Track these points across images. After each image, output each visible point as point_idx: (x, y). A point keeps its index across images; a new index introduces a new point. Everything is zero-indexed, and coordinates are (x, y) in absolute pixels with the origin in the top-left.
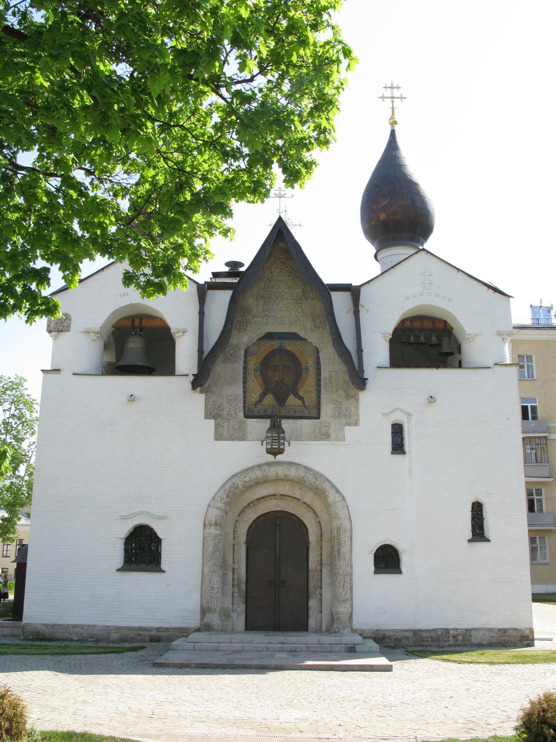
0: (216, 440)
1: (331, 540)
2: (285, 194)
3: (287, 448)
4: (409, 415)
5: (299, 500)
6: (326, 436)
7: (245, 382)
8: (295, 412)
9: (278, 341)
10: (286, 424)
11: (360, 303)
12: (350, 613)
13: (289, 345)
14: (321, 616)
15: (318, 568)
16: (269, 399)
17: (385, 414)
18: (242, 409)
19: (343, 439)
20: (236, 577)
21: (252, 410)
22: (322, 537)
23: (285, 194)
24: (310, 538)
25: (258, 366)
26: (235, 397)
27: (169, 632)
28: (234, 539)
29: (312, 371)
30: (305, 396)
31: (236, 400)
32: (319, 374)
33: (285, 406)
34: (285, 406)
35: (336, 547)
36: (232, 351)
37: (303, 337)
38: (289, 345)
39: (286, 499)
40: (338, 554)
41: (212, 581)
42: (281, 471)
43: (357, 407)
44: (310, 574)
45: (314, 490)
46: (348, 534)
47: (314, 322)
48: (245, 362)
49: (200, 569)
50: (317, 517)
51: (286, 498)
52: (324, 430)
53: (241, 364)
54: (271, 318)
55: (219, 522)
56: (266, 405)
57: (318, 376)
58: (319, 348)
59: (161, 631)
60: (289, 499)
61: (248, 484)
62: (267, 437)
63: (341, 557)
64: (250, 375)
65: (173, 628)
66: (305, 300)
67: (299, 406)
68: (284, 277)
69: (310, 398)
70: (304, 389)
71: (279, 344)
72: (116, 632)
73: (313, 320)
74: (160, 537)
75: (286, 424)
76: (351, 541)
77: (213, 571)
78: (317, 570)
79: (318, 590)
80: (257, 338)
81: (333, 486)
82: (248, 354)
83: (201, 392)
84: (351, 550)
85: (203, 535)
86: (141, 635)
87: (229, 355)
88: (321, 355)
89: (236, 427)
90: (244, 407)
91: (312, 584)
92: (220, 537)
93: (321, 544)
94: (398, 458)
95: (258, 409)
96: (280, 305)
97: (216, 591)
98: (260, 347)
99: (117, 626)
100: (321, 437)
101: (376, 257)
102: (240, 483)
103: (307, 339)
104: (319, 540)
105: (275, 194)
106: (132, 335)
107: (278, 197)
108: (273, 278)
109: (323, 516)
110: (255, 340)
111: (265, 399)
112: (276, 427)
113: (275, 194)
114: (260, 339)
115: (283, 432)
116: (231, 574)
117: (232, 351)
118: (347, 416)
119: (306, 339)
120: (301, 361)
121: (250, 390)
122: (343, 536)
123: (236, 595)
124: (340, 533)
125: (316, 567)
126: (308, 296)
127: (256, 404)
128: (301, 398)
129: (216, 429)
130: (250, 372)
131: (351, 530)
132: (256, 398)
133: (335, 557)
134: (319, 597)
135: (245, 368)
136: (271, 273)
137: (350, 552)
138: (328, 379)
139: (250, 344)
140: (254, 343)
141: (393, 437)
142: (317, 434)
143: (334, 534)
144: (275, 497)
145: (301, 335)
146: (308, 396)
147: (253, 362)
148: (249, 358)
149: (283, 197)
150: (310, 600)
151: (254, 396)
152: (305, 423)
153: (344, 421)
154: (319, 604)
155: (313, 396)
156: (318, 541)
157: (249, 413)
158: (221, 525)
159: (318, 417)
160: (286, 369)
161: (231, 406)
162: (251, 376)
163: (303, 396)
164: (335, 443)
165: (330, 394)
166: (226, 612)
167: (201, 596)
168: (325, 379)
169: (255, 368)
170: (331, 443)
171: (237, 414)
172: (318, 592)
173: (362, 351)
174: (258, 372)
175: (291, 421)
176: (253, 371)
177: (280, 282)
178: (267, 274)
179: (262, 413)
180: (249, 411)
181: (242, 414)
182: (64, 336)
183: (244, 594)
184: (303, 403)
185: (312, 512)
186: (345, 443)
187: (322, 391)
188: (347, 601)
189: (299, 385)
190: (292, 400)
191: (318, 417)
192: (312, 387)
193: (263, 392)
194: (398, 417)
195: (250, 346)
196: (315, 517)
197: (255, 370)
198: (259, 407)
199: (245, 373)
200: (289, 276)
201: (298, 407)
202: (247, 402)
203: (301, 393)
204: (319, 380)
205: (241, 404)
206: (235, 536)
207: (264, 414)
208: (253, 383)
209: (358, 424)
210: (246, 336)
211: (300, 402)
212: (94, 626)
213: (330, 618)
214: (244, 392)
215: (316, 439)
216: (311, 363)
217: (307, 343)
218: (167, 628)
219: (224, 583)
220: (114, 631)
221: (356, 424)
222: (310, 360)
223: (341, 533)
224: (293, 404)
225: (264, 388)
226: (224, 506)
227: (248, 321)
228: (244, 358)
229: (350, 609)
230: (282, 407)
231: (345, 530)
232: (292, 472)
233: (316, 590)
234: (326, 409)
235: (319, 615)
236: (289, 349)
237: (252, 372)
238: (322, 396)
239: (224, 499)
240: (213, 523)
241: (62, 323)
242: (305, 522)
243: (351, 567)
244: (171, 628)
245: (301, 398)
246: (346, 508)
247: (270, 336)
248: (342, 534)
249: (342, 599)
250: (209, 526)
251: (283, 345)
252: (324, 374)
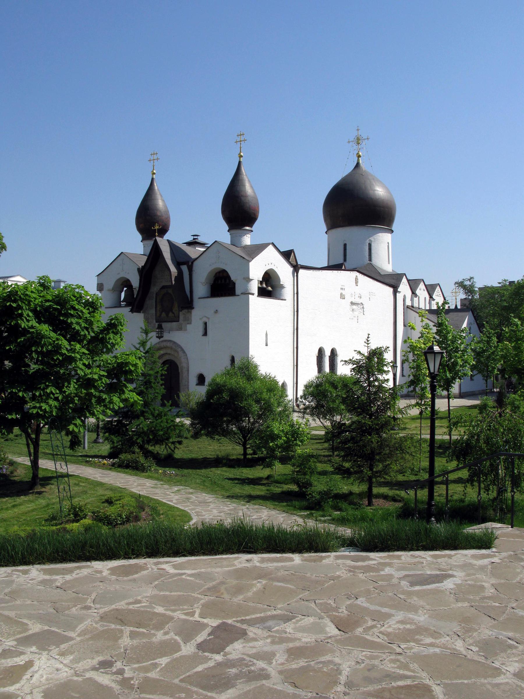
4: (208, 318)
6: (180, 329)
10: (164, 325)
16: (164, 314)
17: (200, 319)
19: (186, 330)
42: (165, 344)
43: (191, 316)
48: (156, 299)
53: (154, 300)
75: (164, 325)
81: (182, 350)
84: (188, 376)
94: (205, 337)
112: (160, 327)
128: (173, 313)
135: (156, 302)
152: (174, 324)
159: (178, 321)
175: (170, 323)
181: (155, 321)
182: (103, 292)
190: (171, 314)
191: (178, 321)
194: (205, 320)
205: (154, 317)
211: (173, 315)
215: (177, 330)
221: (190, 323)
232: (169, 344)
234: (181, 317)
243: (188, 382)
245: (173, 313)
247: (163, 287)
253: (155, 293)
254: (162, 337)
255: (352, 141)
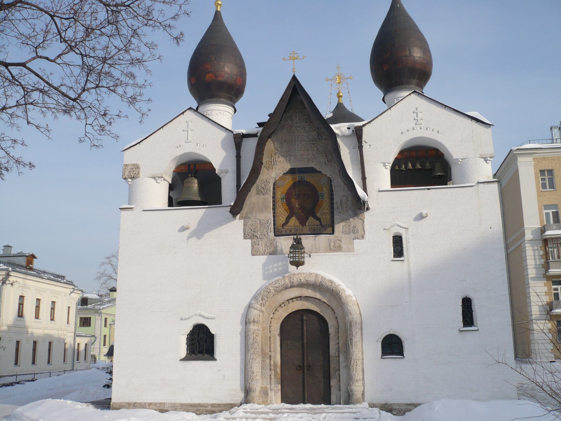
0: (253, 255)
1: (346, 331)
2: (298, 56)
3: (307, 260)
5: (320, 300)
6: (339, 248)
7: (274, 209)
8: (314, 230)
9: (299, 175)
10: (307, 241)
11: (363, 140)
12: (362, 390)
13: (307, 178)
14: (340, 393)
15: (337, 355)
16: (294, 221)
18: (273, 229)
20: (272, 363)
21: (280, 230)
22: (338, 329)
23: (298, 56)
24: (330, 330)
25: (284, 195)
26: (267, 221)
27: (221, 407)
28: (270, 333)
29: (326, 198)
30: (322, 217)
31: (267, 223)
32: (332, 199)
33: (306, 226)
34: (306, 226)
35: (349, 337)
36: (263, 185)
37: (319, 170)
38: (307, 178)
39: (310, 300)
40: (351, 343)
41: (252, 367)
44: (331, 359)
45: (330, 292)
46: (358, 326)
47: (326, 158)
48: (274, 193)
49: (244, 356)
50: (335, 313)
51: (310, 299)
52: (337, 244)
54: (293, 157)
55: (256, 320)
56: (291, 226)
57: (331, 201)
58: (332, 179)
59: (215, 407)
60: (312, 299)
61: (278, 289)
62: (290, 252)
63: (353, 345)
64: (278, 203)
65: (224, 404)
66: (319, 141)
67: (317, 225)
68: (302, 123)
69: (325, 219)
70: (321, 211)
71: (300, 177)
72: (181, 408)
73: (327, 156)
74: (213, 333)
75: (307, 241)
76: (362, 332)
77: (253, 359)
78: (336, 356)
79: (337, 372)
80: (283, 173)
82: (276, 187)
83: (240, 219)
85: (245, 330)
86: (200, 410)
87: (261, 188)
88: (333, 184)
89: (268, 244)
90: (274, 228)
91: (332, 366)
92: (258, 331)
93: (339, 335)
95: (285, 229)
96: (300, 145)
97: (256, 374)
98: (285, 180)
99: (181, 404)
100: (335, 249)
101: (383, 100)
102: (271, 289)
103: (322, 172)
104: (337, 332)
105: (290, 57)
106: (189, 177)
107: (292, 59)
108: (294, 125)
109: (339, 313)
110: (282, 175)
111: (290, 221)
113: (290, 57)
114: (284, 174)
115: (303, 248)
116: (268, 361)
117: (263, 185)
118: (356, 232)
119: (321, 172)
120: (318, 190)
121: (278, 215)
122: (355, 328)
123: (273, 377)
124: (352, 326)
125: (335, 354)
126: (321, 137)
127: (283, 225)
128: (318, 219)
129: (252, 246)
130: (277, 200)
131: (362, 323)
132: (283, 221)
133: (349, 346)
134: (338, 378)
135: (274, 197)
136: (292, 121)
137: (360, 341)
138: (339, 202)
139: (277, 179)
140: (280, 178)
141: (394, 247)
142: (332, 247)
143: (348, 327)
144: (301, 298)
145: (317, 169)
146: (324, 217)
147: (280, 193)
148: (277, 189)
149: (296, 58)
150: (331, 380)
151: (282, 219)
152: (323, 239)
153: (353, 236)
154: (338, 383)
155: (328, 217)
156: (336, 333)
157: (278, 233)
158: (258, 322)
160: (306, 197)
161: (264, 228)
162: (279, 204)
163: (320, 217)
164: (347, 253)
165: (342, 214)
166: (265, 391)
167: (245, 379)
168: (337, 203)
169: (282, 197)
170: (344, 253)
171: (269, 234)
172: (337, 374)
173: (365, 178)
174: (284, 200)
176: (280, 200)
177: (299, 128)
178: (288, 122)
179: (288, 232)
180: (277, 231)
181: (273, 233)
183: (279, 376)
184: (320, 223)
185: (331, 310)
186: (354, 253)
187: (335, 212)
188: (360, 380)
189: (316, 208)
192: (327, 209)
193: (288, 216)
195: (277, 180)
196: (333, 313)
197: (281, 199)
198: (286, 227)
199: (274, 201)
200: (306, 122)
201: (316, 227)
202: (276, 224)
203: (318, 216)
204: (332, 204)
206: (271, 330)
207: (290, 233)
208: (280, 209)
209: (365, 237)
210: (274, 172)
211: (317, 222)
212: (164, 403)
213: (347, 394)
214: (274, 217)
215: (331, 250)
216: (325, 190)
217: (322, 175)
218: (219, 404)
219: (263, 368)
220: (179, 408)
222: (325, 188)
223: (353, 326)
224: (313, 224)
225: (289, 213)
226: (260, 307)
227: (275, 160)
228: (273, 190)
229: (362, 388)
230: (303, 226)
231: (356, 323)
233: (336, 372)
235: (338, 393)
236: (308, 181)
237: (279, 200)
238: (335, 216)
239: (260, 301)
240: (252, 321)
241: (134, 171)
242: (325, 318)
244: (223, 404)
245: (318, 219)
246: (357, 306)
248: (354, 326)
249: (355, 380)
250: (248, 323)
251: (303, 177)
252: (337, 199)
253: (272, 182)
254: (302, 263)
255: (331, 80)
